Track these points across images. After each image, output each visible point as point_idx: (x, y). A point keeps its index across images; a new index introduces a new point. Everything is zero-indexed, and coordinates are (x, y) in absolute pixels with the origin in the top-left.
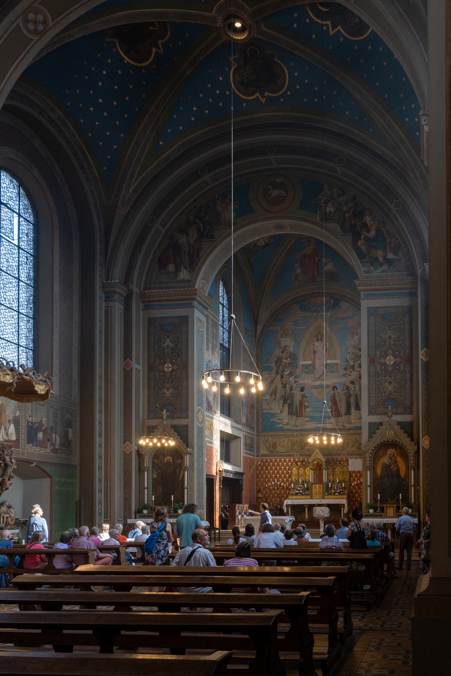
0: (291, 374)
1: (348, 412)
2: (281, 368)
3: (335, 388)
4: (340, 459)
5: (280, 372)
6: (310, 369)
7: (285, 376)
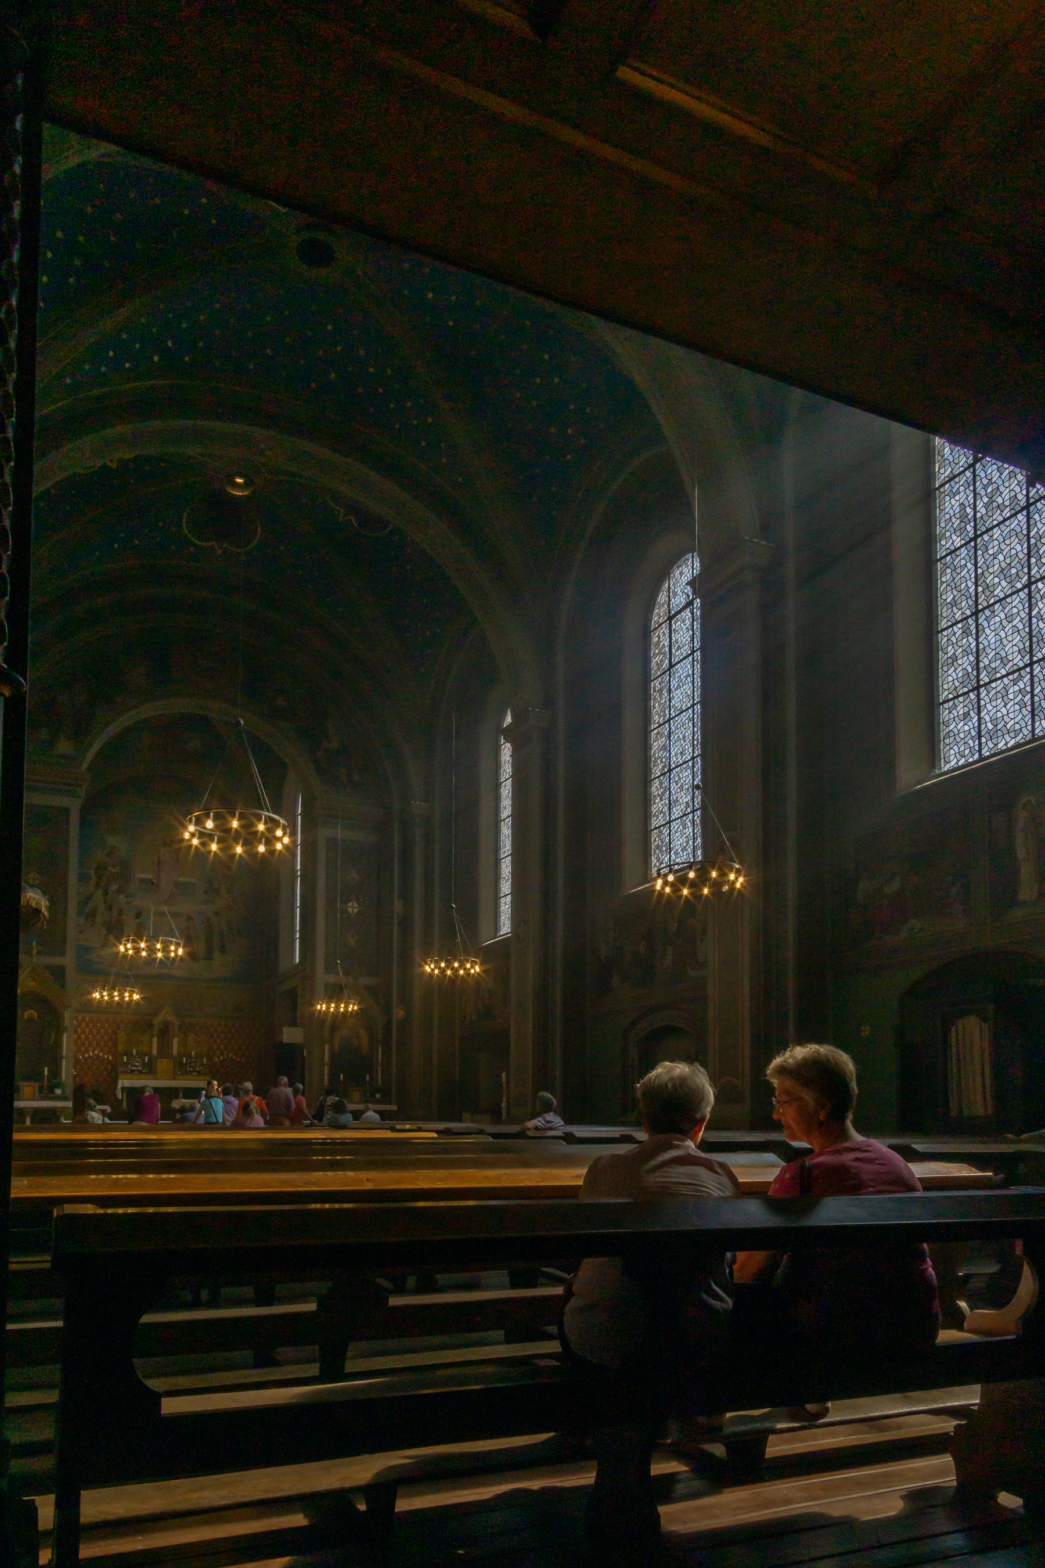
0: (119, 891)
1: (209, 956)
2: (104, 879)
3: (189, 918)
4: (194, 1022)
5: (102, 884)
6: (152, 885)
7: (110, 892)
